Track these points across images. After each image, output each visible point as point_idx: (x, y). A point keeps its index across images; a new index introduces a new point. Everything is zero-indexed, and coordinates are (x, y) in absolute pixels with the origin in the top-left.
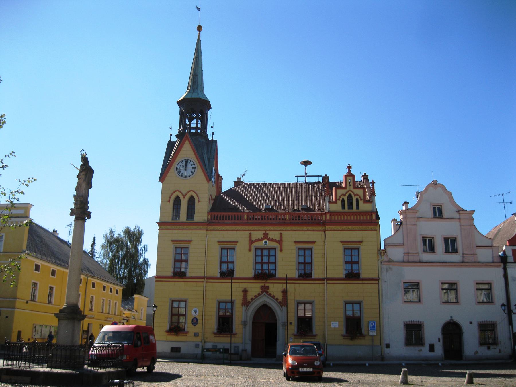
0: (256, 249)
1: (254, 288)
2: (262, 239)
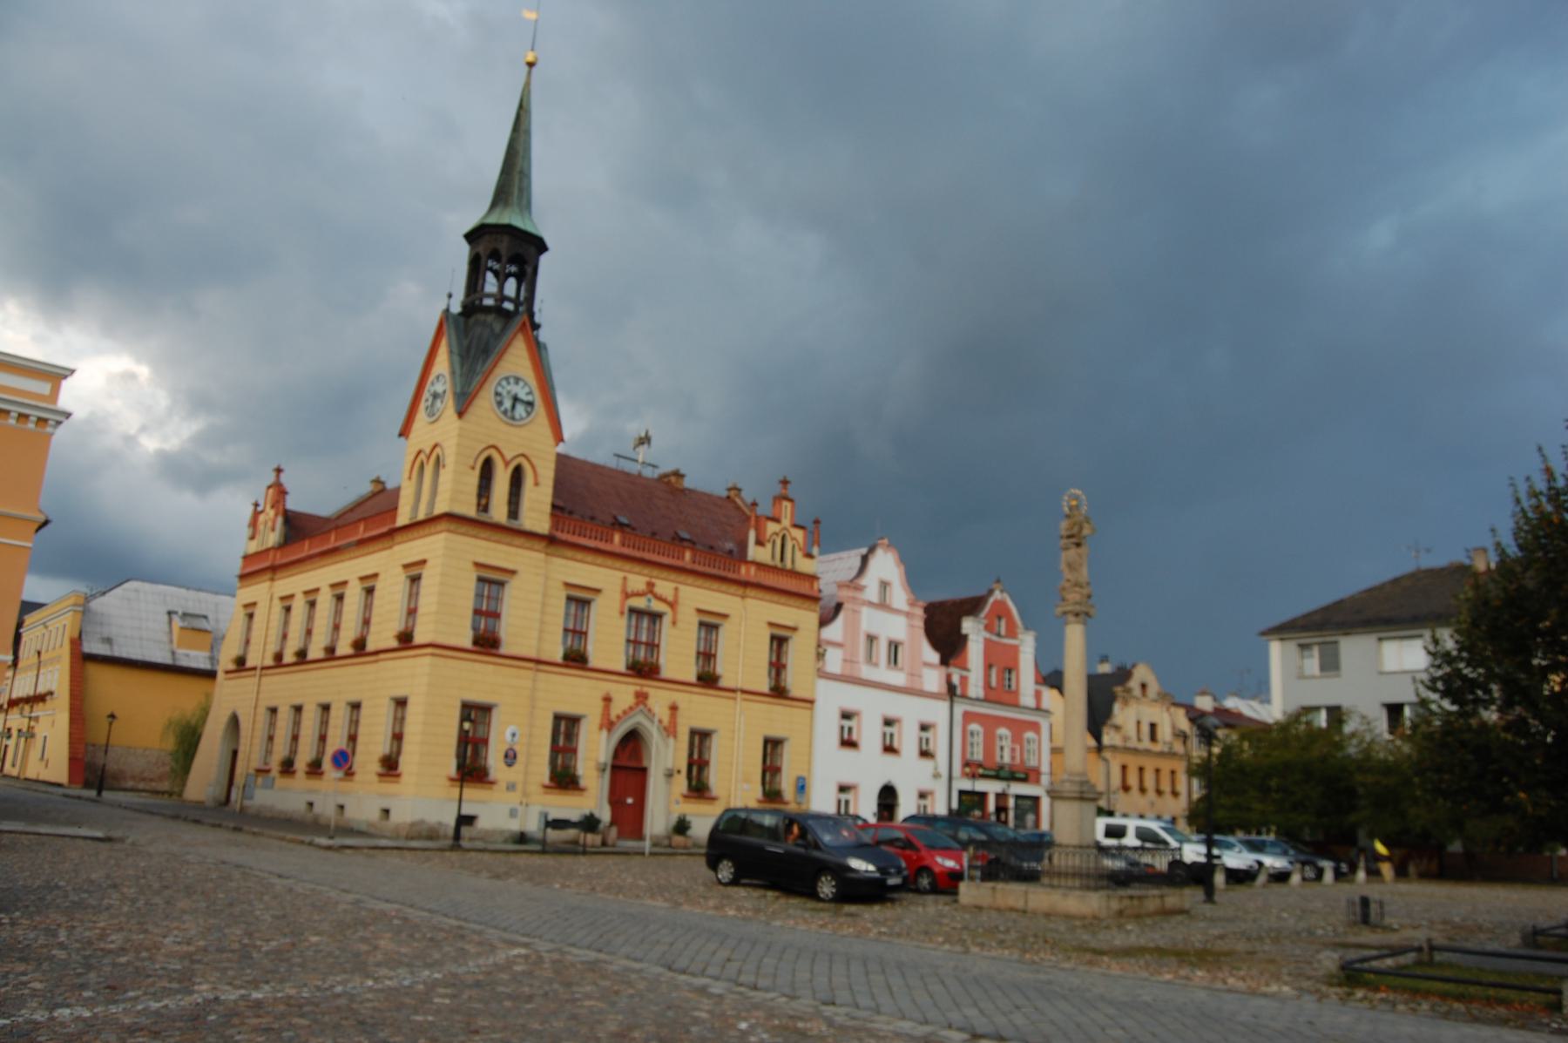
1: (624, 693)
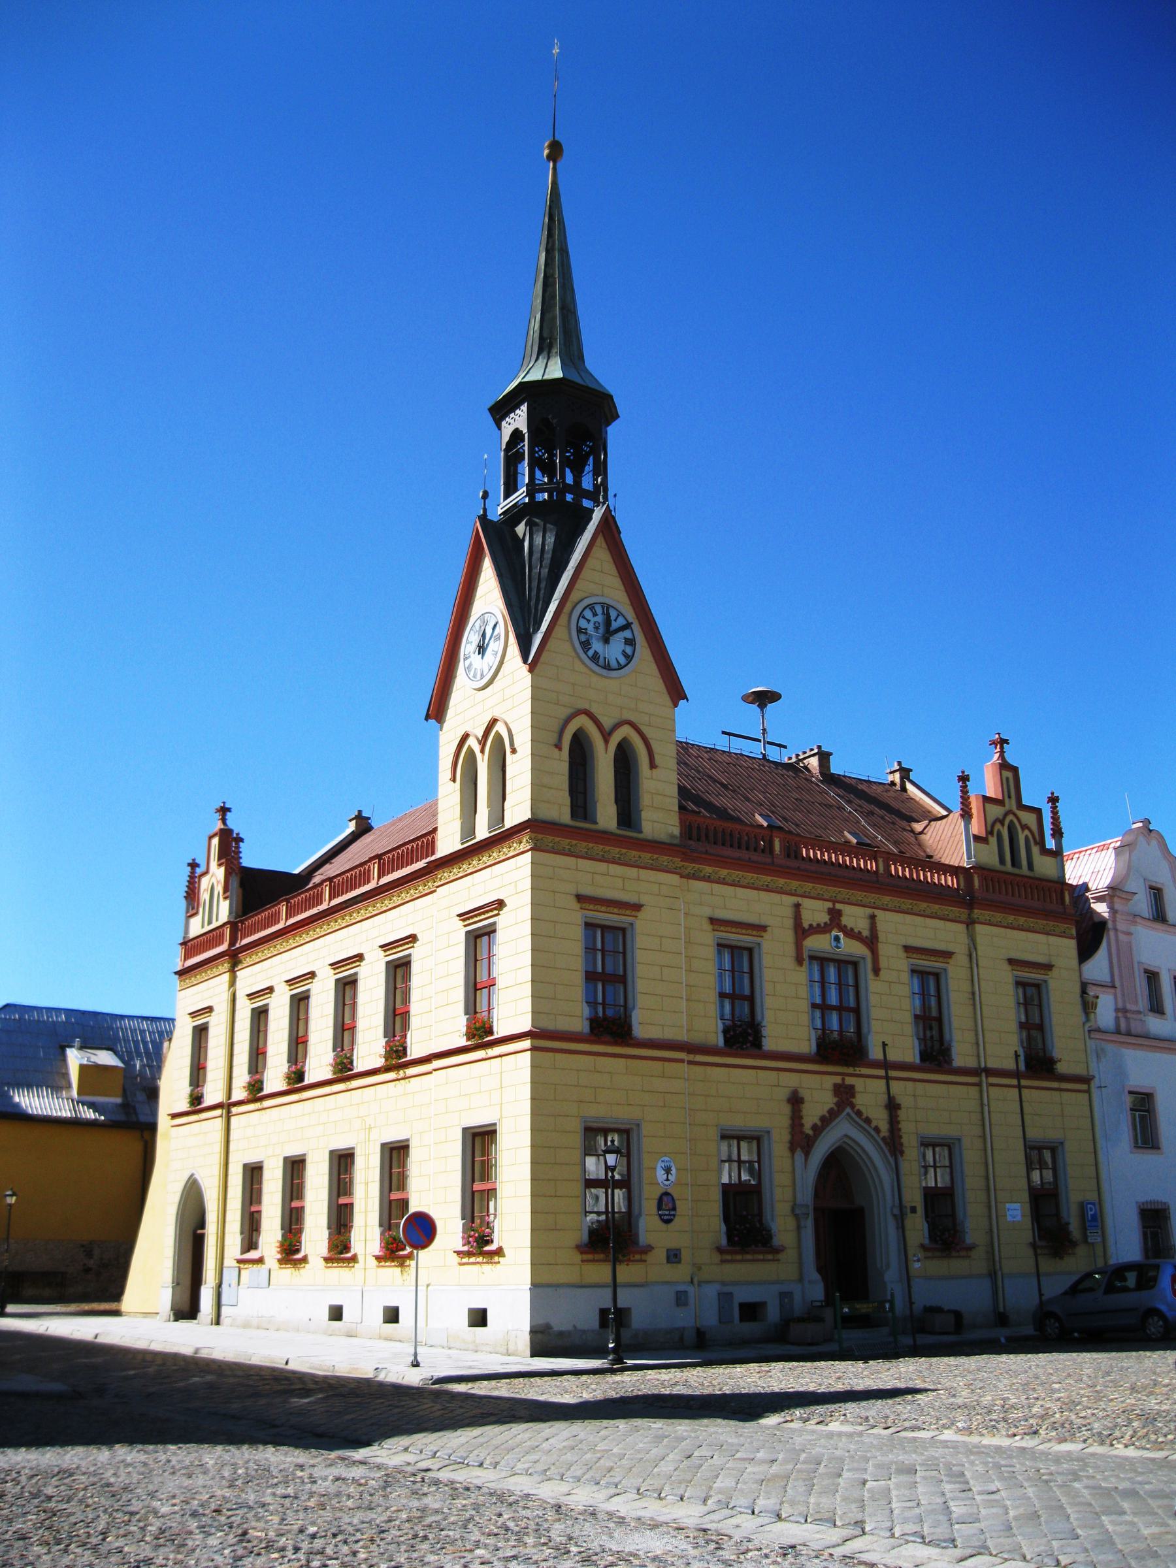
0: (822, 960)
1: (819, 1091)
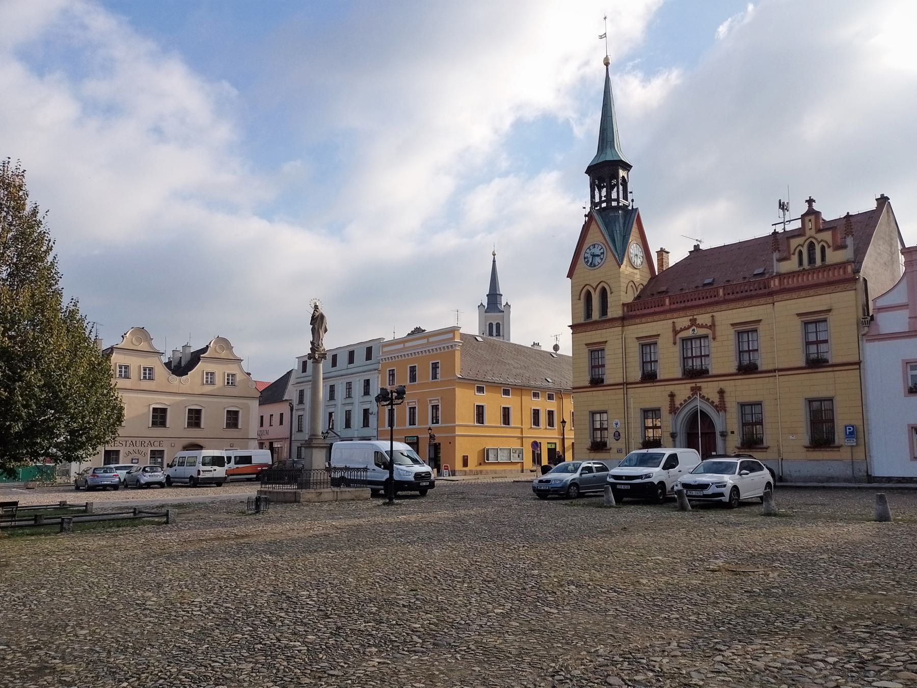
1: (683, 391)
2: (689, 327)
